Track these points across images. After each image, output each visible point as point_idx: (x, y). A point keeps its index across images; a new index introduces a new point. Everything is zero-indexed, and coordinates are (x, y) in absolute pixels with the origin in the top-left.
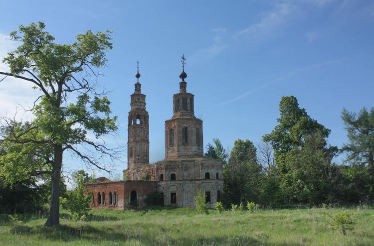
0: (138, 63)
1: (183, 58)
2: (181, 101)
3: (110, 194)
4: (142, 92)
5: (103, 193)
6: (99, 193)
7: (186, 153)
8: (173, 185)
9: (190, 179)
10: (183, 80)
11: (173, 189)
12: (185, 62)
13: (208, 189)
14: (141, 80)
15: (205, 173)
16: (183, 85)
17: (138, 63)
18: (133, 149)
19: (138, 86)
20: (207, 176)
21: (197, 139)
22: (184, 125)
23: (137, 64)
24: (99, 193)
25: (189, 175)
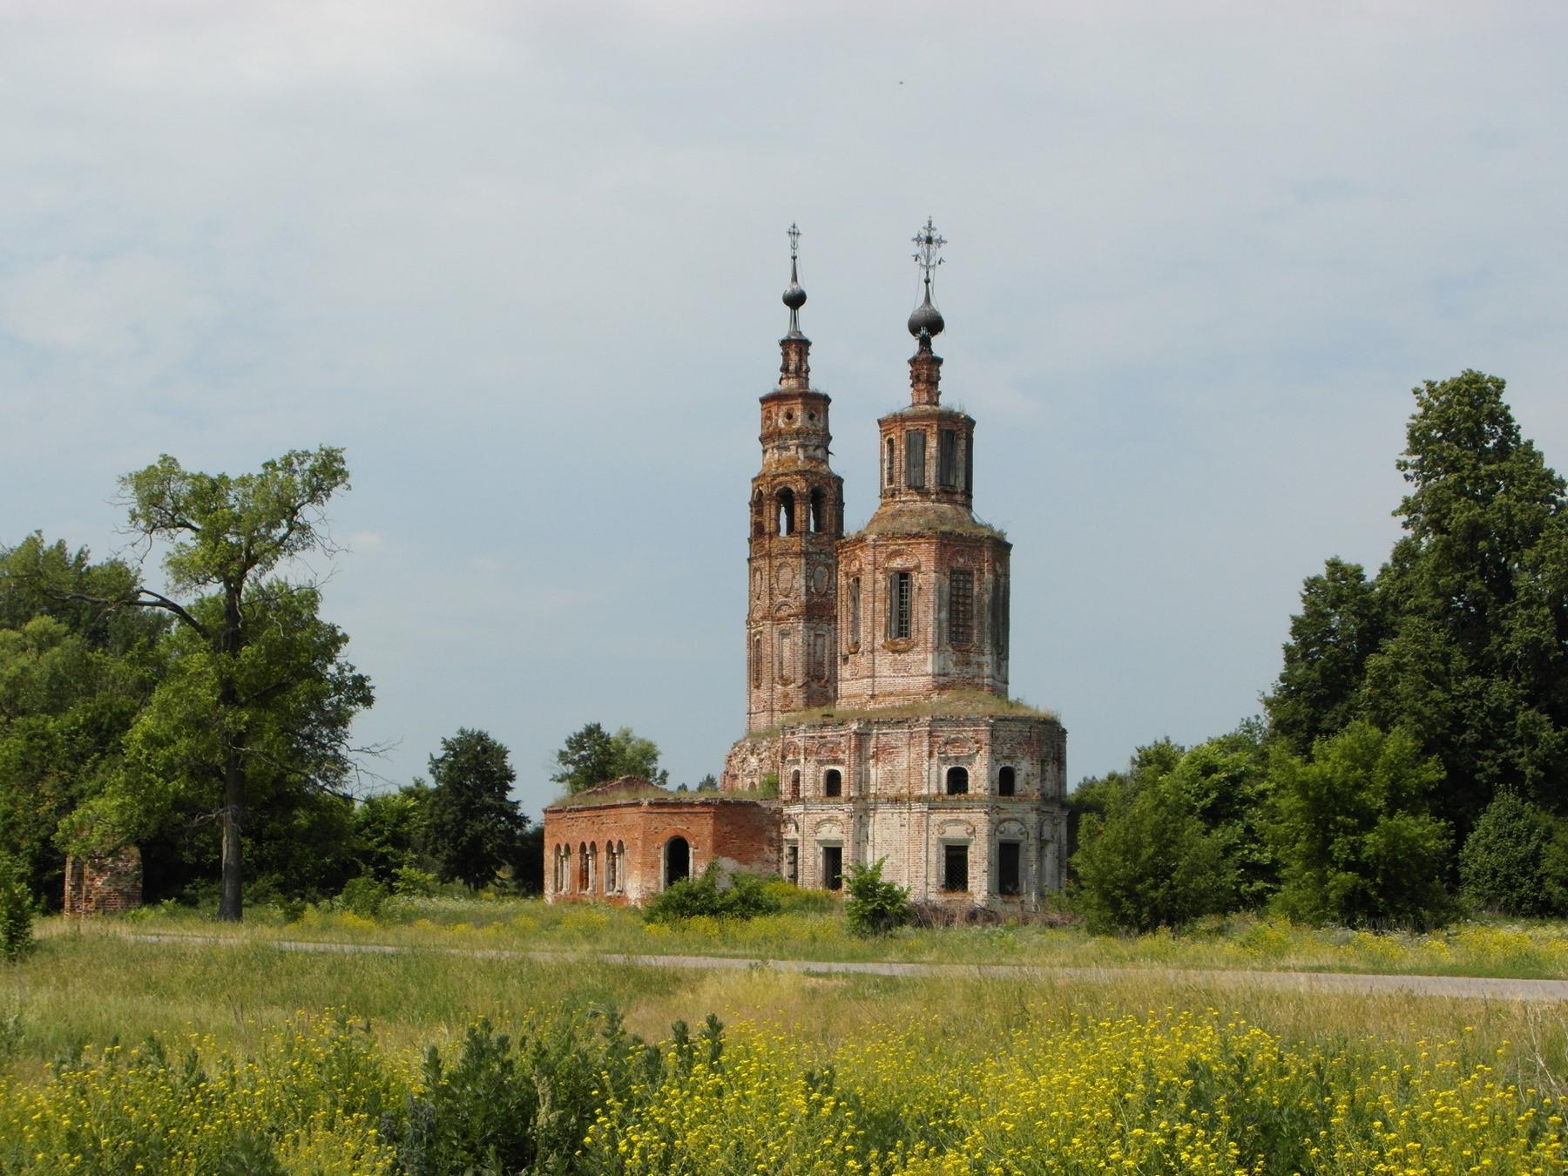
0: (794, 233)
1: (929, 240)
2: (900, 447)
3: (610, 844)
4: (816, 383)
5: (593, 844)
6: (583, 845)
7: (900, 683)
8: (829, 820)
9: (892, 792)
10: (925, 343)
11: (831, 833)
12: (938, 252)
13: (956, 833)
14: (809, 321)
15: (945, 770)
16: (926, 370)
17: (794, 233)
18: (766, 649)
19: (796, 346)
20: (958, 780)
21: (950, 619)
22: (897, 563)
23: (788, 239)
24: (583, 845)
25: (891, 778)
